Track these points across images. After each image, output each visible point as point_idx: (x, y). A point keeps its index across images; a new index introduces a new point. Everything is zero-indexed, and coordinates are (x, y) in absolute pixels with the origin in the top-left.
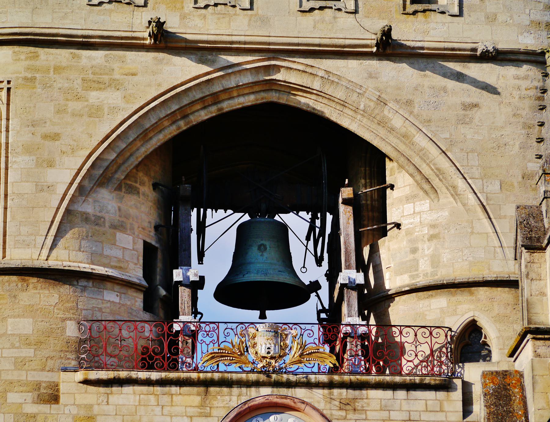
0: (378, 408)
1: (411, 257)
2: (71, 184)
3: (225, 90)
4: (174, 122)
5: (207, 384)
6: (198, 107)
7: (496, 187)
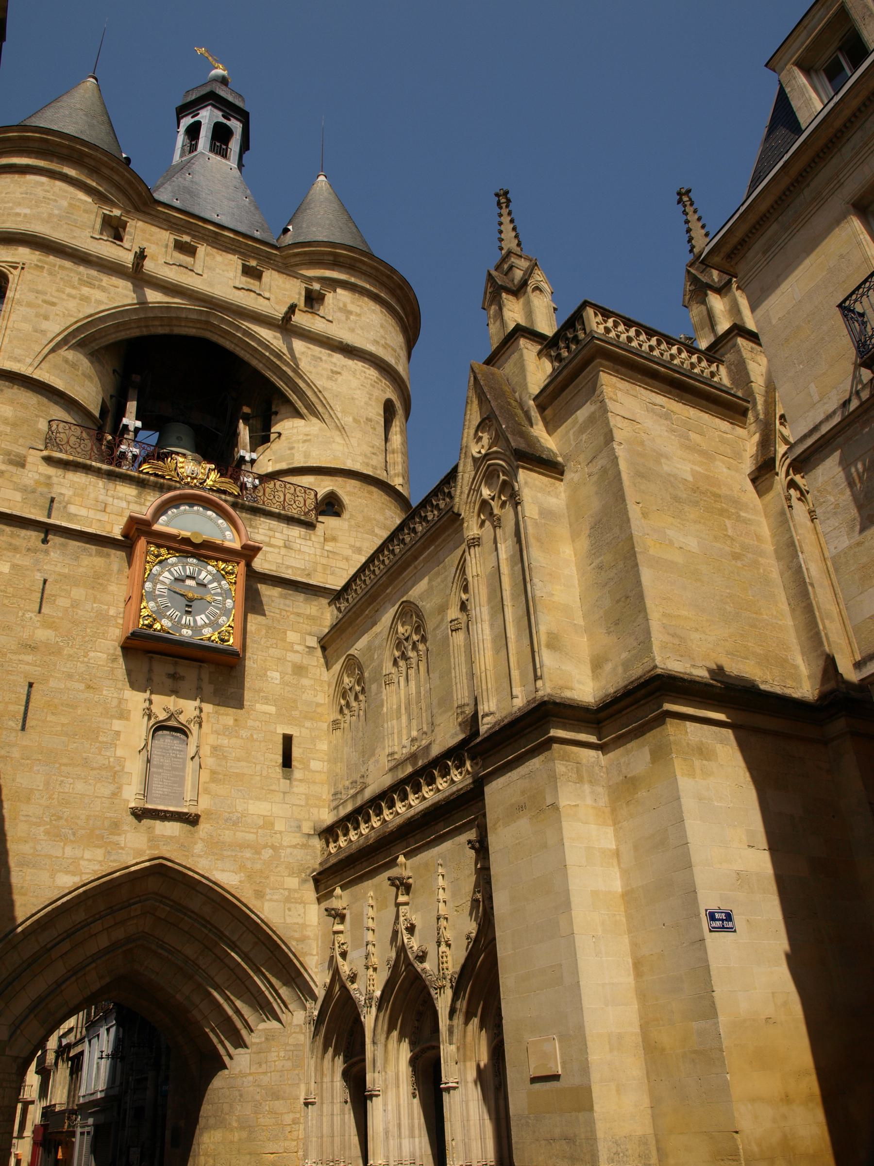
0: (267, 528)
1: (289, 452)
2: (59, 335)
3: (178, 318)
4: (138, 327)
5: (141, 484)
6: (157, 323)
7: (351, 419)
